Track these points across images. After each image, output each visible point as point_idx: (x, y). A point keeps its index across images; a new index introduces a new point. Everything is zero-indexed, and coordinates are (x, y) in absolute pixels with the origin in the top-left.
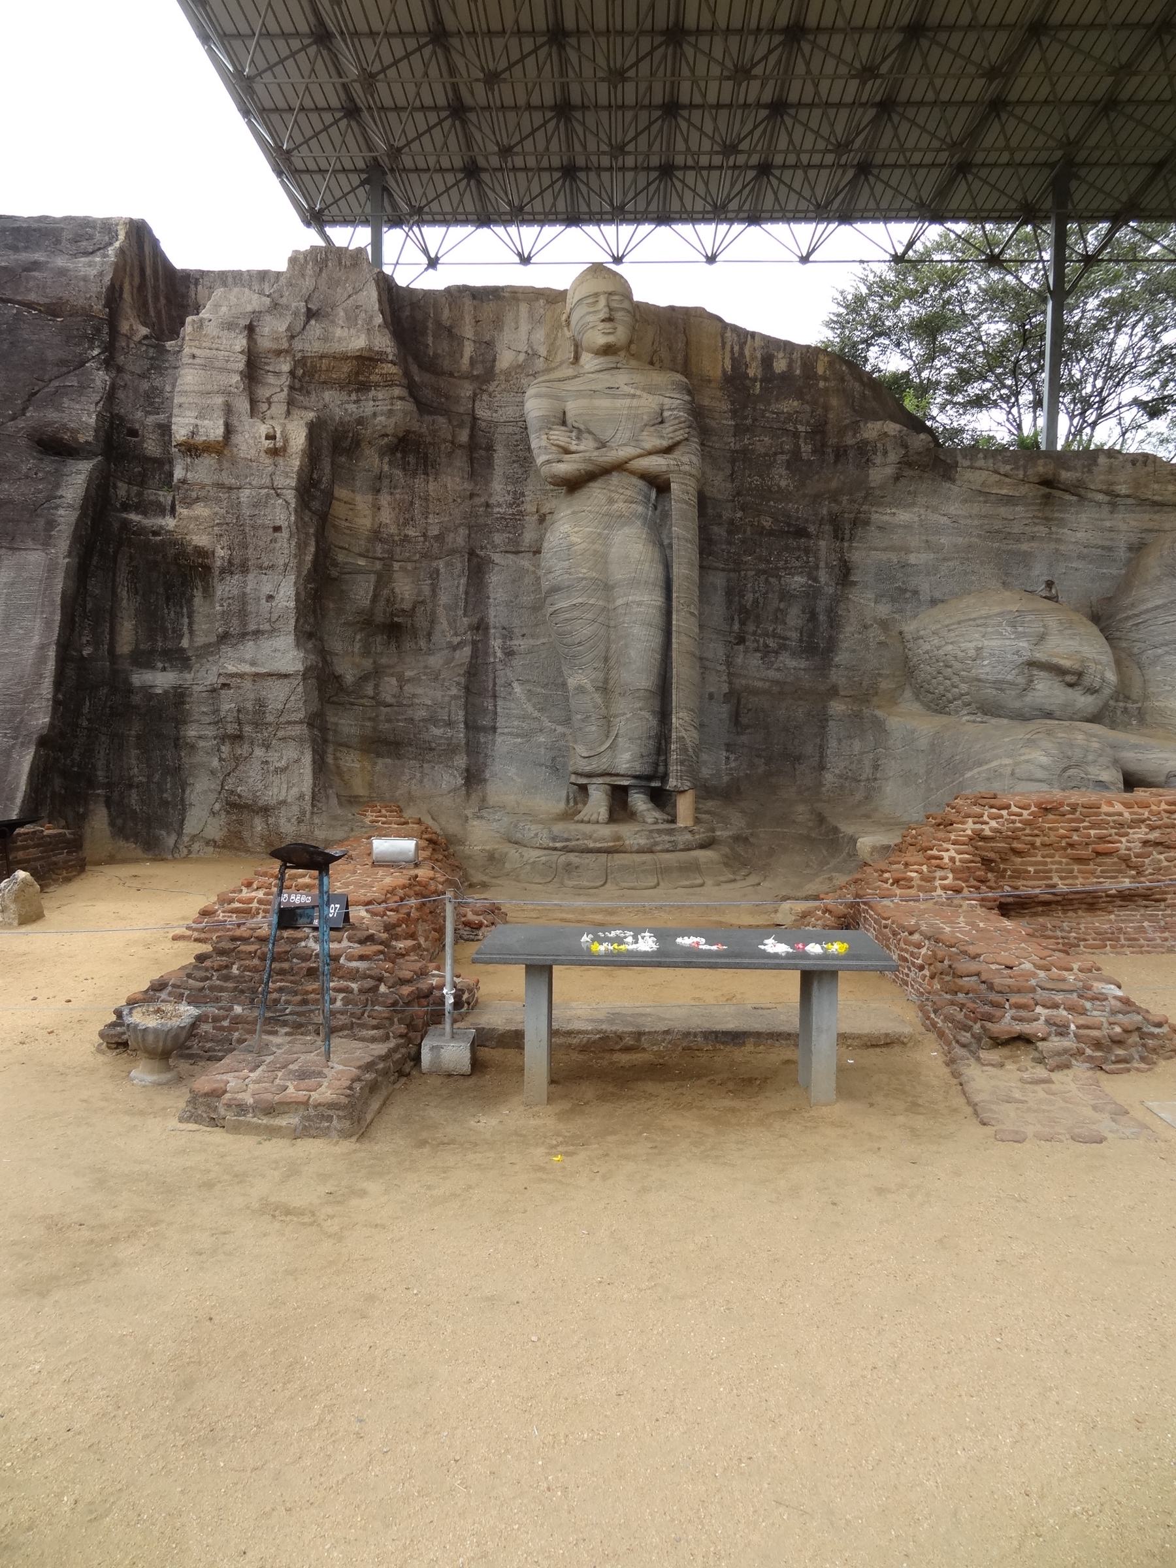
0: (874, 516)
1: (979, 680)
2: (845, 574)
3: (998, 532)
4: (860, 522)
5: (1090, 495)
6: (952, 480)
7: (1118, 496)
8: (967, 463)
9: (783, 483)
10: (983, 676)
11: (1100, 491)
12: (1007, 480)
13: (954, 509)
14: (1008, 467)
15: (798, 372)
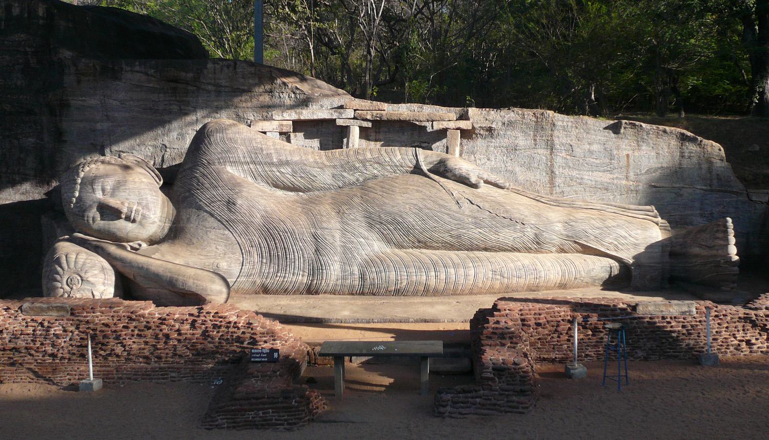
0: (72, 102)
1: (77, 215)
2: (59, 136)
3: (150, 109)
4: (64, 105)
5: (203, 87)
6: (120, 80)
7: (222, 86)
8: (129, 68)
9: (19, 83)
10: (77, 213)
11: (209, 84)
12: (153, 79)
13: (122, 96)
14: (153, 71)
15: (26, 15)
